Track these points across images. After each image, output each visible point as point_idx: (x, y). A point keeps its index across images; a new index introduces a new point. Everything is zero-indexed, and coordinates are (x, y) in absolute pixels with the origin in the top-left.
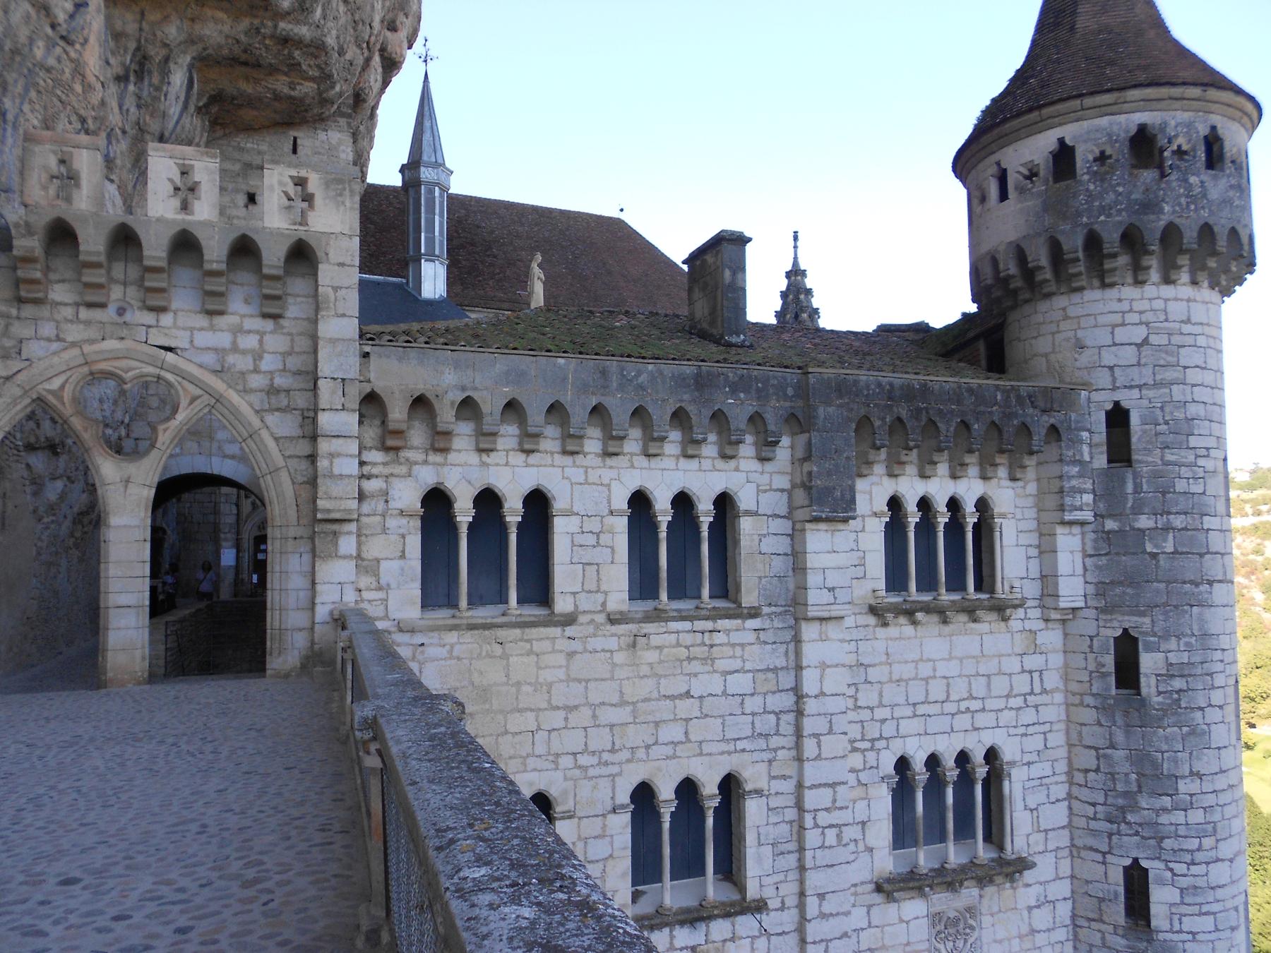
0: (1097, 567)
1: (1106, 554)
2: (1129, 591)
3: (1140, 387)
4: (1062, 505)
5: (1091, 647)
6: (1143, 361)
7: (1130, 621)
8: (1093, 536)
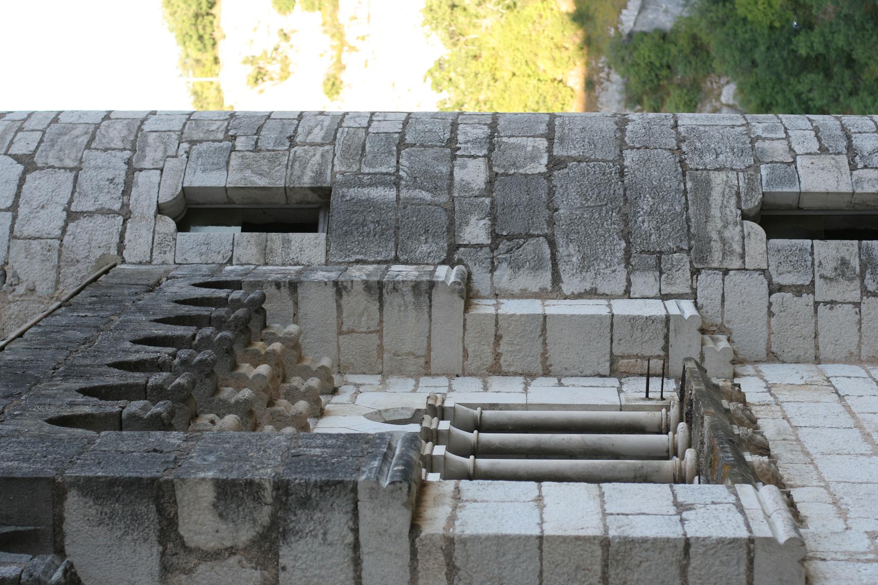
0: (585, 265)
1: (552, 244)
2: (646, 204)
3: (132, 170)
4: (416, 287)
5: (798, 290)
6: (71, 164)
7: (722, 206)
8: (503, 274)
